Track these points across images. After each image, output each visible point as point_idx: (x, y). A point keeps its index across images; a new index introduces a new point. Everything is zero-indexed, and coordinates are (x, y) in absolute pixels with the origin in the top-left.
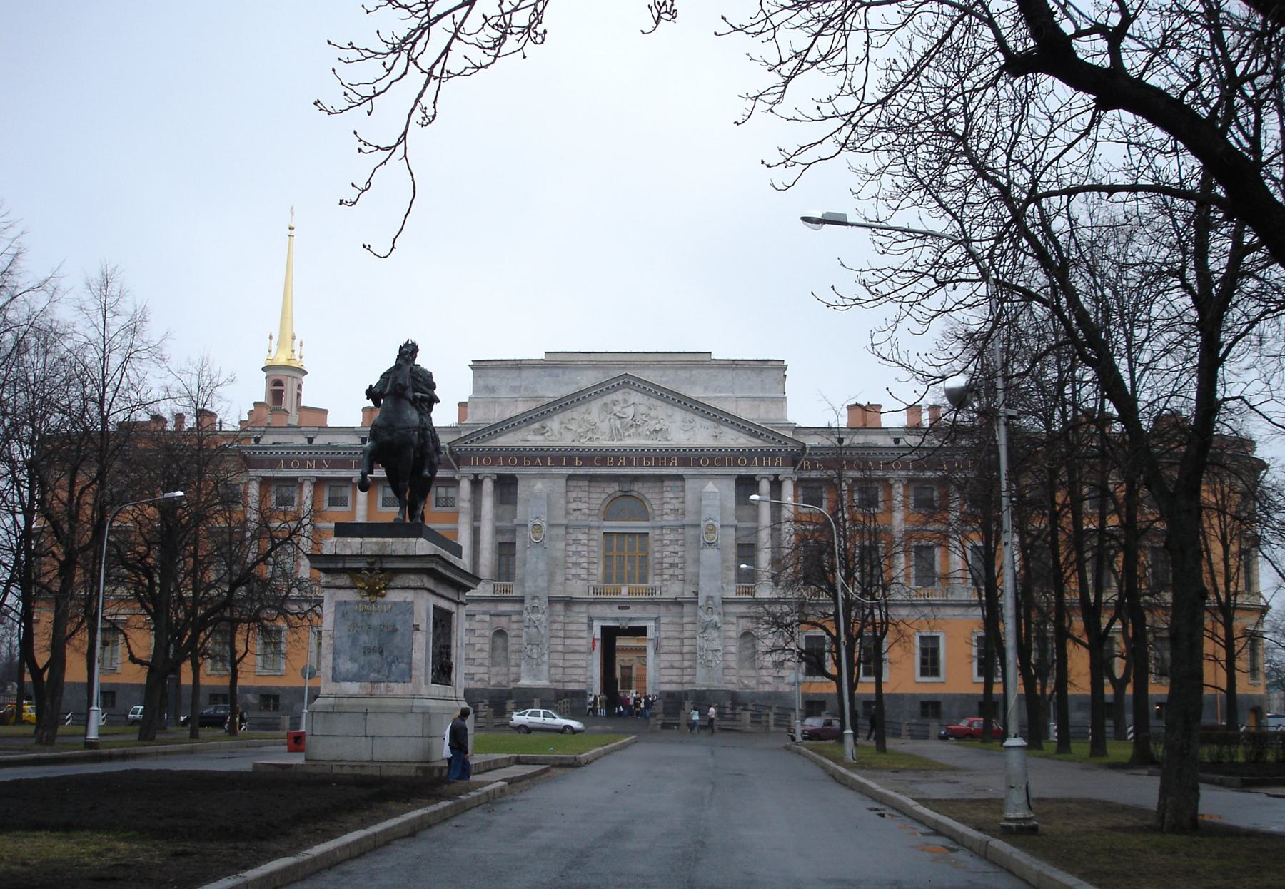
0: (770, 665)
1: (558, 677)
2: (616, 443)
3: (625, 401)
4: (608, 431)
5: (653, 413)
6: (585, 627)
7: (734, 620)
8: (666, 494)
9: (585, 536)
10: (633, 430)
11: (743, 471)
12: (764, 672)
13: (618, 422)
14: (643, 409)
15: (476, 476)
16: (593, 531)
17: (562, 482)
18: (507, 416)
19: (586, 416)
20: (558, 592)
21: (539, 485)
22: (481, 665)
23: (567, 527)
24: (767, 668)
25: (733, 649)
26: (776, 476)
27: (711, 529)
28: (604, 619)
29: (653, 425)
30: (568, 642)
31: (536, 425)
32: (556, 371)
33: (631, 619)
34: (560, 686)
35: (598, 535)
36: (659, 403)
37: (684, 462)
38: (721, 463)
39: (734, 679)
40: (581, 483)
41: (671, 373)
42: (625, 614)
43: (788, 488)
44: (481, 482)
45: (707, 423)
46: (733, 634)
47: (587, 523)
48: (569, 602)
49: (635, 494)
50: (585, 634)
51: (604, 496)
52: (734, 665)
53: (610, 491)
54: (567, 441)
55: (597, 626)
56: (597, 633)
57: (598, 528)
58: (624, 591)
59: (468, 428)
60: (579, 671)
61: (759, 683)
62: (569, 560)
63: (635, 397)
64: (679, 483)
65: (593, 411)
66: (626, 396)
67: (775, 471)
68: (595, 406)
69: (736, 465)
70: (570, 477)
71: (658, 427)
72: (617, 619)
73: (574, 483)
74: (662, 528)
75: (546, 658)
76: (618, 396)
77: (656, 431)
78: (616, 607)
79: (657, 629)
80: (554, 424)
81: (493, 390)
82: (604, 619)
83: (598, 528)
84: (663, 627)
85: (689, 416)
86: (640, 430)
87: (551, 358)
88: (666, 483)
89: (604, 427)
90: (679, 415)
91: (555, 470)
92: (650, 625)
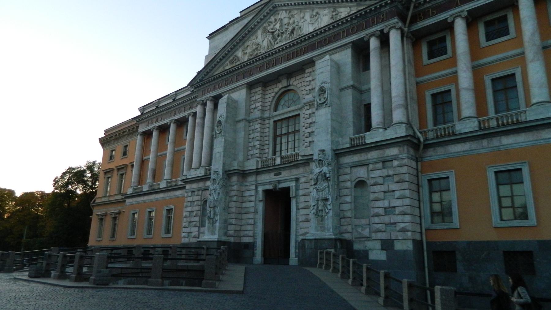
0: (381, 211)
1: (231, 232)
4: (266, 45)
6: (253, 193)
7: (348, 170)
9: (258, 126)
11: (354, 38)
12: (376, 220)
14: (286, 21)
15: (203, 101)
16: (267, 122)
20: (235, 166)
22: (195, 226)
24: (377, 215)
25: (348, 199)
26: (382, 31)
27: (322, 90)
28: (263, 184)
30: (244, 205)
31: (231, 58)
33: (279, 182)
34: (232, 240)
36: (296, 12)
37: (312, 48)
38: (336, 37)
39: (349, 229)
40: (258, 89)
42: (278, 178)
43: (395, 38)
45: (326, 11)
46: (349, 184)
48: (244, 174)
49: (291, 87)
50: (253, 198)
51: (273, 94)
52: (348, 214)
53: (276, 90)
55: (260, 189)
56: (260, 196)
57: (269, 118)
58: (278, 161)
60: (250, 228)
61: (371, 232)
62: (250, 145)
66: (276, 17)
67: (379, 27)
68: (259, 32)
69: (348, 35)
70: (250, 86)
72: (270, 183)
75: (217, 218)
76: (272, 19)
77: (292, 32)
78: (272, 174)
79: (297, 189)
80: (239, 54)
82: (263, 184)
83: (269, 118)
84: (302, 186)
86: (284, 36)
87: (243, 13)
88: (307, 71)
89: (265, 44)
91: (238, 84)
92: (293, 184)
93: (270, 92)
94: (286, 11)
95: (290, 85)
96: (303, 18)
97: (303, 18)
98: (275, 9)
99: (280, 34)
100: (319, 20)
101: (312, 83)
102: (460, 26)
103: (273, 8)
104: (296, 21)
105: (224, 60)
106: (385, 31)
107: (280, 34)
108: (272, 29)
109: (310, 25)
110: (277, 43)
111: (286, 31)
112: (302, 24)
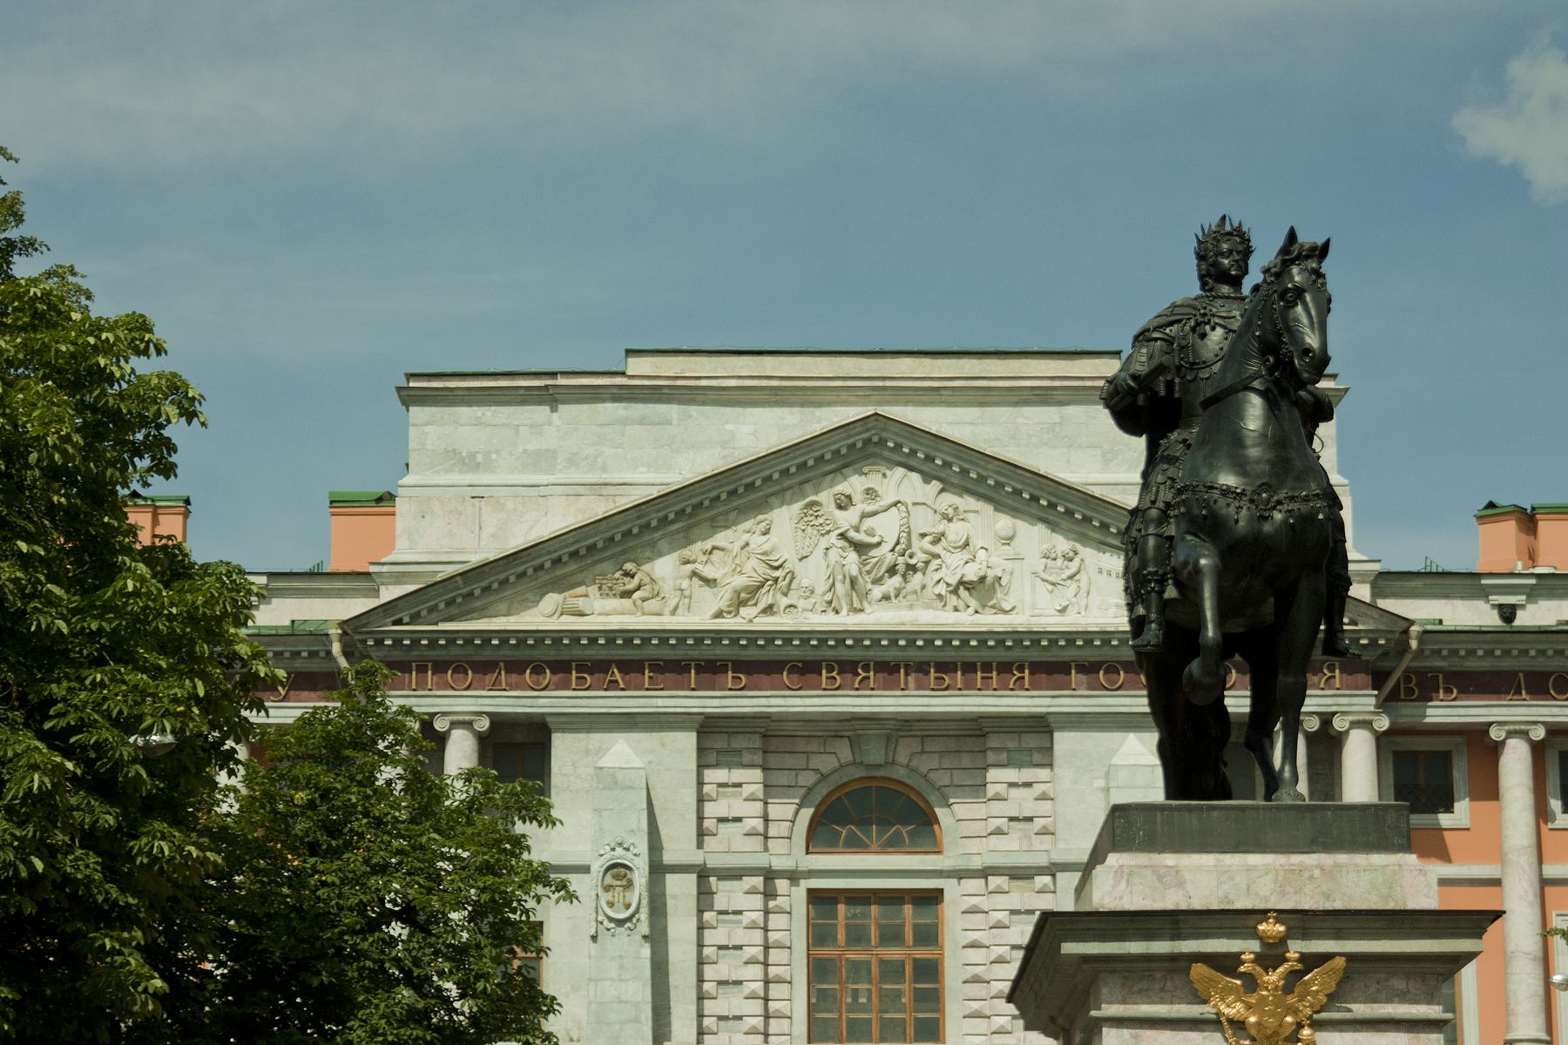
2: (846, 621)
3: (870, 493)
4: (822, 587)
5: (955, 531)
8: (992, 774)
10: (897, 579)
13: (852, 556)
14: (924, 521)
17: (686, 741)
18: (518, 540)
19: (757, 541)
21: (621, 750)
23: (703, 873)
29: (955, 567)
32: (662, 408)
35: (794, 897)
40: (739, 742)
41: (1003, 414)
44: (441, 739)
47: (761, 860)
51: (807, 779)
53: (826, 763)
54: (699, 614)
57: (794, 876)
59: (399, 578)
63: (899, 484)
64: (1032, 741)
65: (780, 531)
66: (873, 480)
71: (971, 573)
73: (720, 742)
74: (985, 873)
81: (470, 463)
83: (794, 876)
85: (1062, 544)
88: (993, 741)
89: (813, 574)
90: (1034, 538)
93: (790, 761)
94: (927, 478)
95: (893, 763)
96: (1008, 540)
97: (1008, 540)
98: (871, 449)
99: (901, 568)
100: (1083, 577)
101: (1015, 793)
102: (1515, 765)
103: (867, 442)
104: (977, 542)
105: (572, 567)
106: (1339, 724)
107: (901, 568)
108: (857, 529)
109: (1043, 588)
110: (886, 598)
111: (927, 563)
112: (1009, 565)
